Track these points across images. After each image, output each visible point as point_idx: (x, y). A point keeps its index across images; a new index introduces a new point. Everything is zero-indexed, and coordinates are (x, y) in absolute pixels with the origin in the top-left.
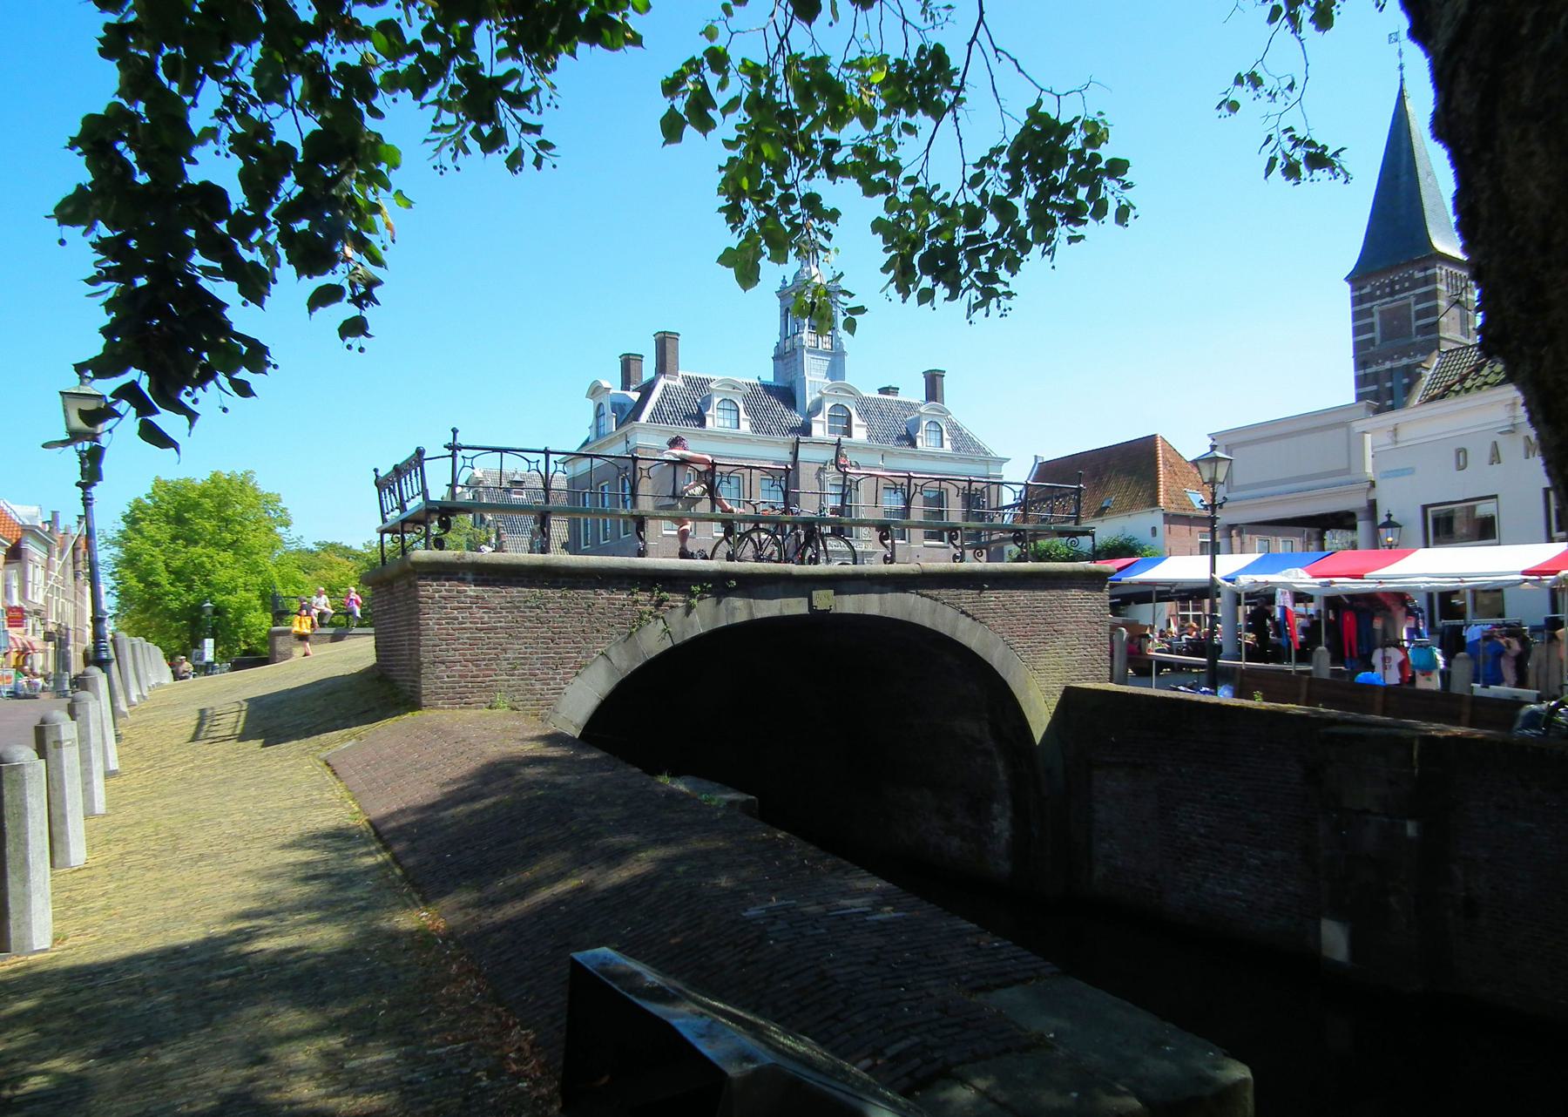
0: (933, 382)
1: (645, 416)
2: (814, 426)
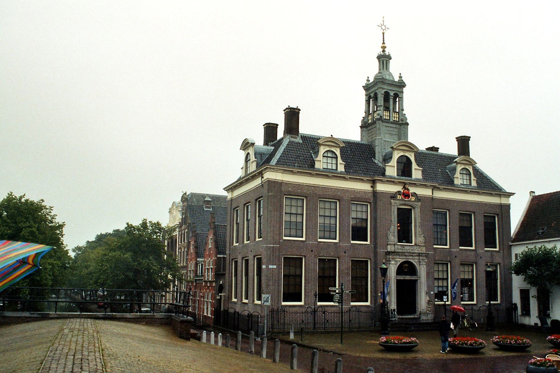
0: (463, 143)
1: (274, 161)
2: (387, 169)
